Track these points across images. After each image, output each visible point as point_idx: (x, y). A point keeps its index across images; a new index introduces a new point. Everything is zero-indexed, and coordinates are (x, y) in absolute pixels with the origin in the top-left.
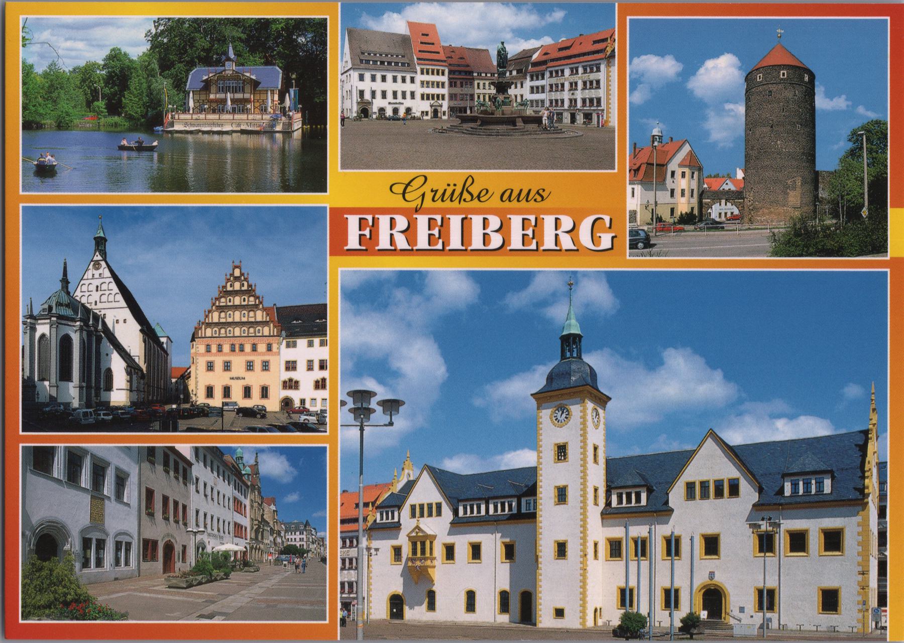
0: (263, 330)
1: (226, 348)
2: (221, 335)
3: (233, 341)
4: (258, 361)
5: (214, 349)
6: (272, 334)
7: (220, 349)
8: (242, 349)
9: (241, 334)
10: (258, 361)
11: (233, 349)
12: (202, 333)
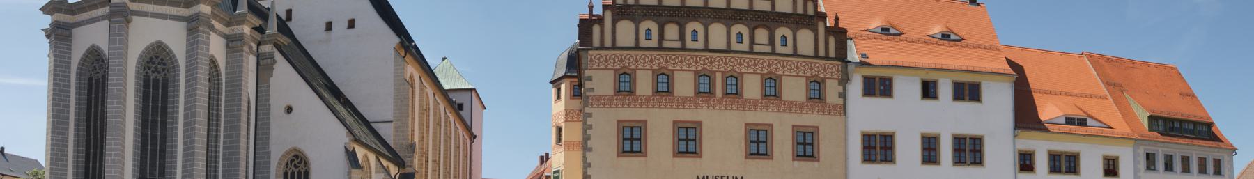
0: (795, 40)
1: (684, 84)
2: (666, 44)
3: (704, 62)
4: (782, 126)
5: (644, 85)
6: (822, 53)
7: (664, 90)
8: (734, 94)
9: (729, 43)
10: (782, 126)
11: (704, 92)
12: (602, 32)
